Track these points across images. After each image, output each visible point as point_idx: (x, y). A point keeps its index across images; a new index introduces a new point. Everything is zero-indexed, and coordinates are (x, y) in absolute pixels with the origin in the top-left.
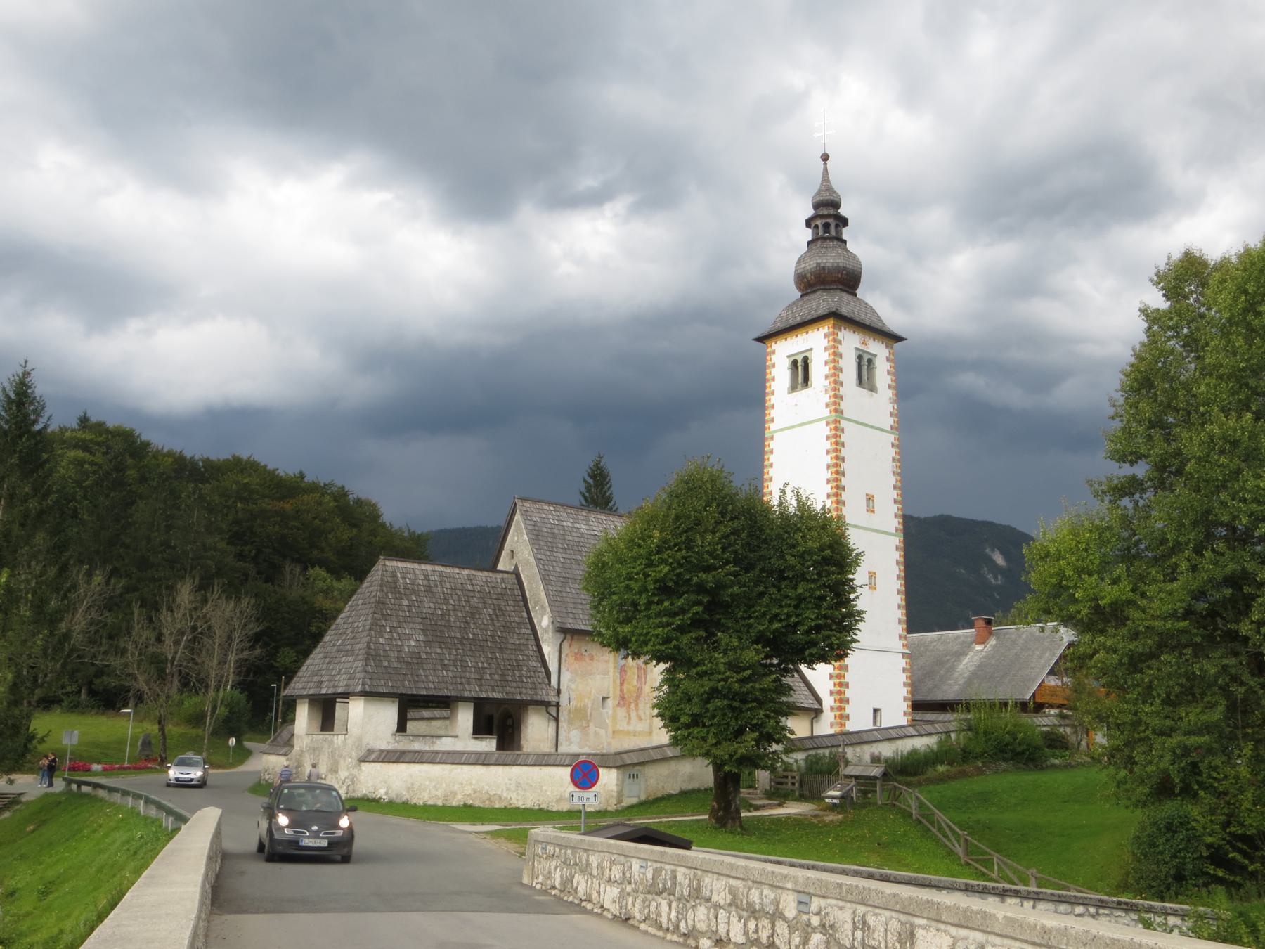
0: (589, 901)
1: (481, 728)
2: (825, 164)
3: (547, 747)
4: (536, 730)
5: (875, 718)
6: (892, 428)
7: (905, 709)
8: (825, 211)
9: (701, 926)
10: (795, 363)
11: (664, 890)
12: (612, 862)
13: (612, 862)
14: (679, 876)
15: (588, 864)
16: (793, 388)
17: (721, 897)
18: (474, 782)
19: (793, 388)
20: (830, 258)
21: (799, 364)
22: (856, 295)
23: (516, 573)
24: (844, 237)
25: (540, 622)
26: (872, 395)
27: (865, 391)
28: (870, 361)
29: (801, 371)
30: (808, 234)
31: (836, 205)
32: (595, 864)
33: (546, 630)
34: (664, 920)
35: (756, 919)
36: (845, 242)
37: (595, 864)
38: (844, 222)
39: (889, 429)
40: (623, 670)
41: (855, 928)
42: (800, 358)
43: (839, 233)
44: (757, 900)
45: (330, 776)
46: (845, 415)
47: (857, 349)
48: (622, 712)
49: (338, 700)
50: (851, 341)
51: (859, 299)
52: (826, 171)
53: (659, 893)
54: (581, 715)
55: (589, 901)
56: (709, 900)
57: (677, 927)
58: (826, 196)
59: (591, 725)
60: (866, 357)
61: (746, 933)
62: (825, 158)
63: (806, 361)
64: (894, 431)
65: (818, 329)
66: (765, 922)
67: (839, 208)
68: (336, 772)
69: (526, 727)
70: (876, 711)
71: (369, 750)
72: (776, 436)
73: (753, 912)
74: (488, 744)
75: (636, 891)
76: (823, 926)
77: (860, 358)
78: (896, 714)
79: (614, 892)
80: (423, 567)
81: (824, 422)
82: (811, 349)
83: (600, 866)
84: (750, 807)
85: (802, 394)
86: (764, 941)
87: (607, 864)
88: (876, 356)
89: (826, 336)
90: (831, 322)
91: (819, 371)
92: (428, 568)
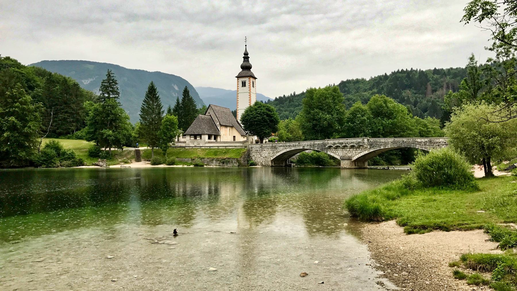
4: (219, 139)
8: (246, 56)
10: (243, 83)
16: (243, 86)
19: (243, 86)
20: (246, 64)
23: (210, 115)
29: (244, 84)
31: (247, 54)
33: (218, 125)
38: (249, 57)
40: (225, 130)
42: (244, 82)
50: (252, 79)
52: (246, 48)
58: (246, 53)
62: (246, 46)
63: (245, 82)
67: (248, 54)
74: (215, 141)
85: (244, 88)
91: (247, 84)
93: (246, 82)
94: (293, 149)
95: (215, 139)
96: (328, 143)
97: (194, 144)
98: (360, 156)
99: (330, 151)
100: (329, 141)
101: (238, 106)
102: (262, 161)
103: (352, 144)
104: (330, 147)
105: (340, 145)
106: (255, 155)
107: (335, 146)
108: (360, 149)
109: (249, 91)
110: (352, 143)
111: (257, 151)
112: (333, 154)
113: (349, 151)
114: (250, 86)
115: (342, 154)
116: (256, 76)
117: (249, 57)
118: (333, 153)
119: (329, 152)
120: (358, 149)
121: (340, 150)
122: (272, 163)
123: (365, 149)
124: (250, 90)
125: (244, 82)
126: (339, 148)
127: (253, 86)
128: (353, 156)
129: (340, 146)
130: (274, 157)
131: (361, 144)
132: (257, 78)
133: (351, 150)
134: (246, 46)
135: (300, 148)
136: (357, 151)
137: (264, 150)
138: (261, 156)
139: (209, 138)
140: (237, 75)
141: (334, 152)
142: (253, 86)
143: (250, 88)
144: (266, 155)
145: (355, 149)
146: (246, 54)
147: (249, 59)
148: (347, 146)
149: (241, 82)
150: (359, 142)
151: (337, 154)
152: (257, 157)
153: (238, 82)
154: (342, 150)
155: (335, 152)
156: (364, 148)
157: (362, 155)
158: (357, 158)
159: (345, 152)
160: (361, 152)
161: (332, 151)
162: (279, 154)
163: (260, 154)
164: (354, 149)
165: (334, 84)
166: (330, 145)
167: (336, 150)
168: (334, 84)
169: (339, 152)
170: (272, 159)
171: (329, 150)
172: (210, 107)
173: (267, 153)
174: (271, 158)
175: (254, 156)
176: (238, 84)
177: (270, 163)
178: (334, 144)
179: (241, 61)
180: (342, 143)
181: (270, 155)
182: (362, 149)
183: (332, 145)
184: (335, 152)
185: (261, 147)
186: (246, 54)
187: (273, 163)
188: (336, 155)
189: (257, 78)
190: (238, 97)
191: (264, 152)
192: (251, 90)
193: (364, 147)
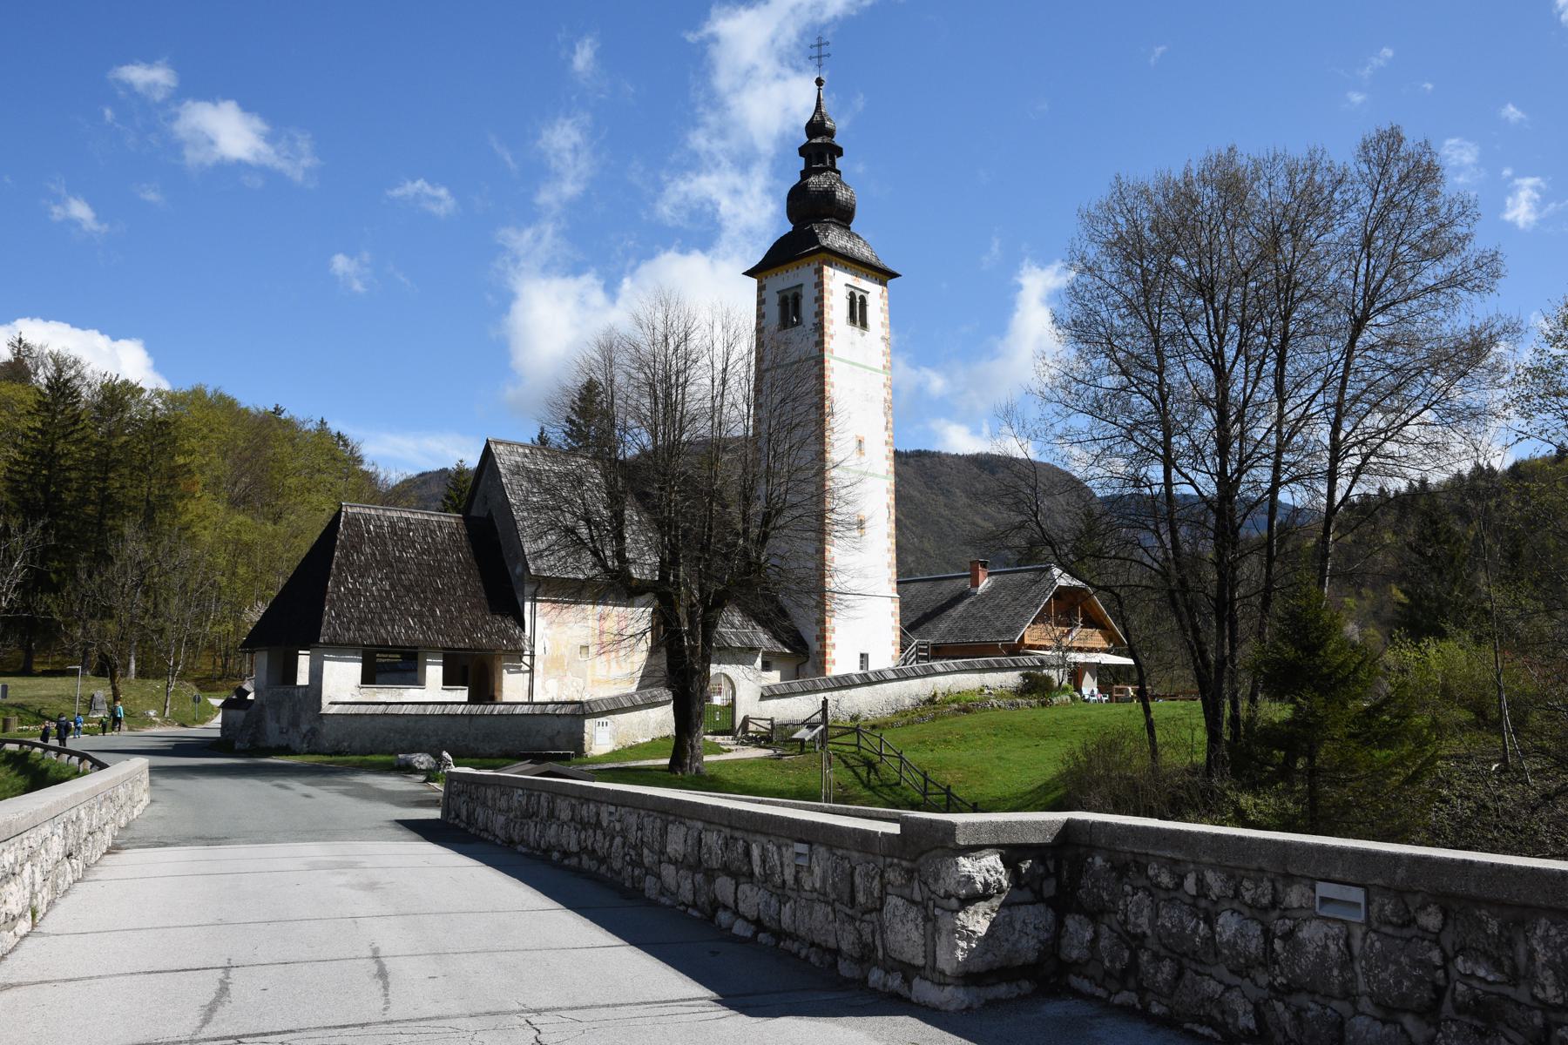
0: (486, 830)
1: (449, 680)
2: (819, 89)
5: (862, 662)
6: (884, 367)
7: (893, 653)
9: (553, 841)
11: (534, 813)
12: (502, 794)
13: (502, 794)
14: (542, 799)
15: (486, 797)
17: (565, 815)
18: (440, 733)
21: (790, 301)
22: (849, 229)
24: (837, 167)
25: (514, 570)
26: (863, 335)
27: (857, 330)
28: (863, 299)
30: (800, 163)
32: (490, 796)
34: (531, 839)
35: (586, 831)
36: (838, 172)
37: (490, 796)
38: (839, 151)
39: (881, 369)
41: (638, 829)
42: (790, 294)
43: (833, 163)
44: (586, 815)
45: (291, 730)
46: (835, 355)
47: (847, 285)
49: (300, 652)
51: (852, 234)
53: (530, 817)
54: (556, 663)
55: (486, 830)
56: (558, 819)
57: (539, 845)
59: (569, 674)
60: (858, 294)
61: (579, 843)
63: (797, 299)
64: (887, 371)
65: (809, 265)
66: (590, 832)
68: (298, 726)
70: (862, 655)
71: (331, 703)
73: (584, 825)
74: (462, 694)
75: (516, 817)
76: (622, 829)
77: (852, 295)
78: (885, 655)
79: (501, 819)
80: (388, 513)
82: (801, 285)
83: (494, 799)
84: (718, 749)
85: (792, 333)
86: (590, 848)
87: (498, 795)
88: (868, 293)
90: (824, 255)
92: (395, 514)
93: (805, 291)
114: (820, 314)
117: (839, 151)
140: (757, 258)
143: (819, 328)
153: (760, 302)
192: (830, 344)
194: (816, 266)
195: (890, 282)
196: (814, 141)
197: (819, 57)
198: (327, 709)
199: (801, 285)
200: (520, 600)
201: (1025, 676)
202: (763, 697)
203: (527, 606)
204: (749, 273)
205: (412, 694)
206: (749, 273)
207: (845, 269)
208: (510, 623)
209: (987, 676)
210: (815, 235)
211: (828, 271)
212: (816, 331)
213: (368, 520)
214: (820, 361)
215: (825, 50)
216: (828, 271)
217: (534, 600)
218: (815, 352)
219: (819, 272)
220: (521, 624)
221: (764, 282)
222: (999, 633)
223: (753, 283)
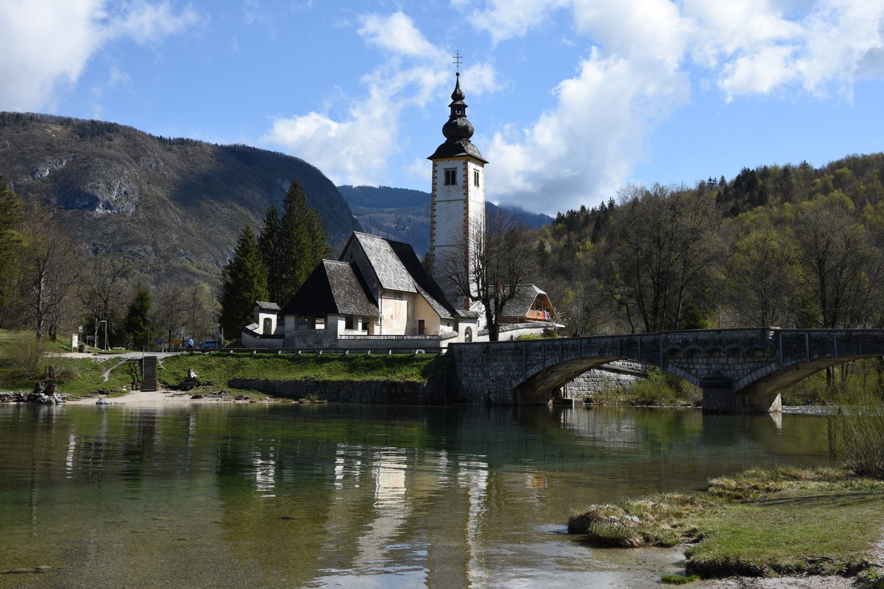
3: (378, 334)
4: (377, 330)
10: (447, 173)
16: (447, 183)
21: (450, 174)
38: (467, 106)
42: (451, 171)
48: (395, 321)
52: (458, 83)
60: (477, 172)
62: (458, 74)
63: (454, 173)
69: (373, 328)
72: (437, 203)
74: (366, 333)
77: (475, 172)
81: (463, 201)
82: (456, 168)
85: (451, 188)
89: (464, 163)
90: (468, 157)
91: (459, 178)
94: (573, 357)
95: (365, 328)
96: (668, 341)
97: (305, 342)
98: (755, 378)
99: (673, 365)
100: (669, 336)
101: (434, 238)
102: (486, 392)
103: (733, 346)
104: (674, 352)
105: (701, 348)
106: (470, 374)
107: (689, 350)
108: (757, 360)
109: (464, 197)
110: (731, 342)
111: (475, 362)
112: (683, 372)
113: (727, 363)
114: (466, 181)
115: (706, 372)
116: (484, 157)
117: (467, 106)
118: (682, 368)
119: (670, 366)
120: (749, 359)
121: (700, 361)
122: (515, 396)
123: (769, 359)
124: (466, 194)
125: (451, 171)
126: (698, 355)
127: (477, 183)
128: (737, 378)
129: (699, 351)
130: (521, 380)
131: (757, 346)
132: (488, 163)
133: (731, 361)
134: (458, 74)
135: (593, 355)
136: (746, 366)
137: (495, 360)
138: (486, 376)
139: (350, 326)
141: (686, 366)
142: (477, 183)
143: (466, 187)
144: (500, 373)
145: (741, 360)
146: (457, 96)
147: (466, 109)
148: (719, 351)
149: (443, 172)
150: (752, 339)
151: (694, 371)
152: (475, 380)
153: (434, 172)
154: (705, 361)
155: (688, 368)
156: (768, 357)
157: (760, 376)
158: (747, 384)
159: (713, 366)
160: (758, 368)
161: (680, 365)
162: (534, 372)
163: (482, 370)
164: (739, 357)
165: (723, 178)
166: (673, 347)
167: (690, 361)
168: (723, 178)
169: (697, 367)
170: (515, 384)
171: (671, 361)
172: (354, 239)
173: (503, 368)
174: (513, 381)
175: (466, 375)
176: (434, 178)
177: (510, 398)
178: (686, 343)
179: (446, 114)
180: (705, 343)
181: (511, 373)
182: (762, 359)
183: (678, 347)
184: (688, 368)
185: (484, 352)
186: (457, 96)
187: (519, 397)
188: (690, 376)
189: (488, 163)
190: (435, 213)
191: (495, 364)
192: (470, 194)
193: (767, 355)
194: (464, 161)
195: (485, 165)
196: (457, 103)
197: (458, 63)
198: (339, 337)
199: (456, 168)
200: (376, 298)
201: (544, 330)
202: (479, 335)
203: (379, 300)
204: (429, 158)
205: (355, 333)
206: (429, 158)
207: (473, 162)
208: (373, 306)
209: (532, 330)
210: (463, 147)
211: (469, 163)
212: (464, 188)
213: (331, 265)
214: (466, 201)
215: (460, 60)
216: (469, 163)
217: (381, 298)
218: (464, 197)
219: (466, 164)
220: (377, 306)
221: (436, 163)
222: (518, 313)
223: (431, 162)
